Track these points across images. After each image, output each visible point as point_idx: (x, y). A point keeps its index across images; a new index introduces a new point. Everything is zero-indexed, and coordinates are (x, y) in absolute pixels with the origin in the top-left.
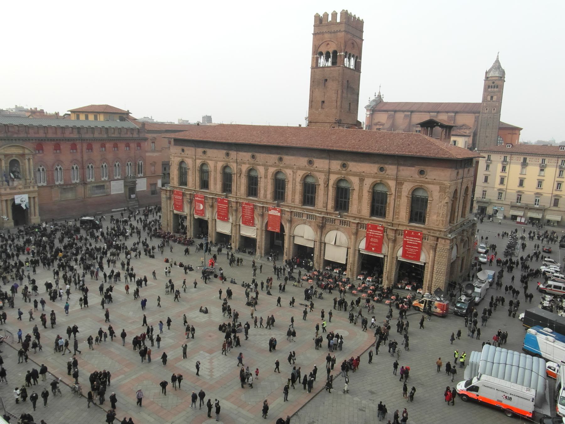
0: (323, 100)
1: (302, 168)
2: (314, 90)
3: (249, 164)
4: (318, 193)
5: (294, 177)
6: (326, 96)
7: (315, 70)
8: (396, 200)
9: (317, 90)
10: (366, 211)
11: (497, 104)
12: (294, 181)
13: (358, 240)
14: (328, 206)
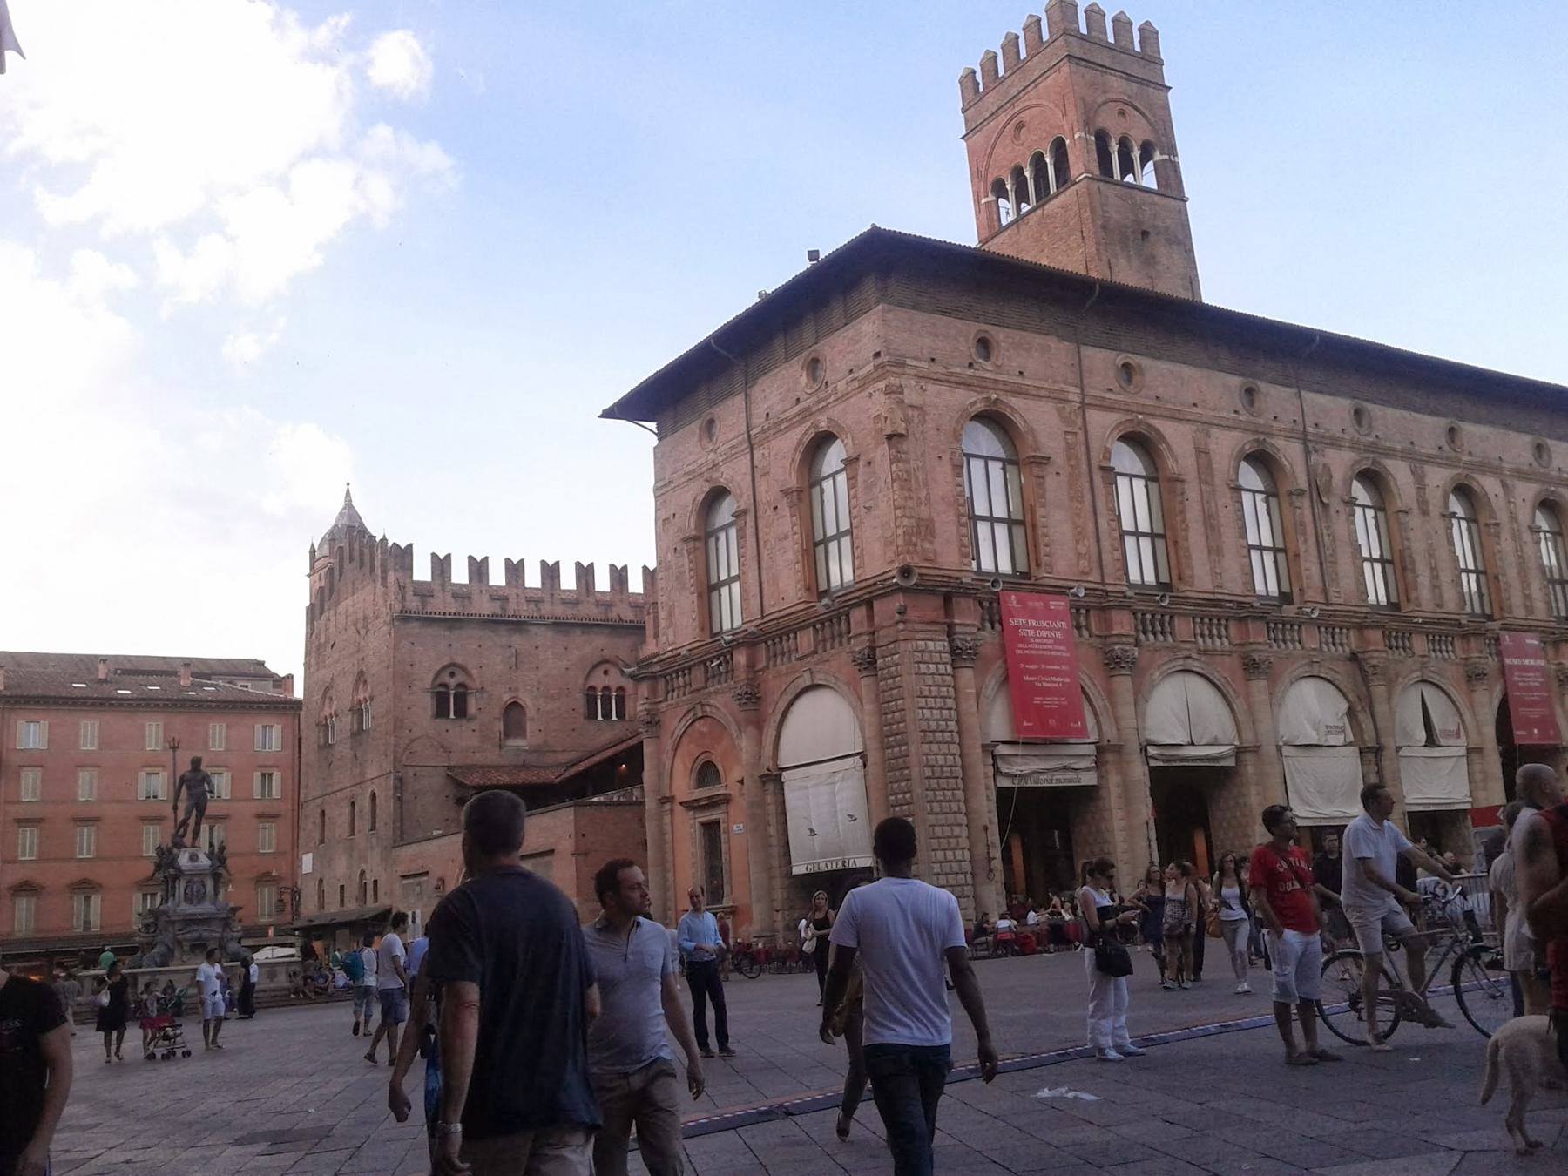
2: (1113, 261)
3: (1354, 446)
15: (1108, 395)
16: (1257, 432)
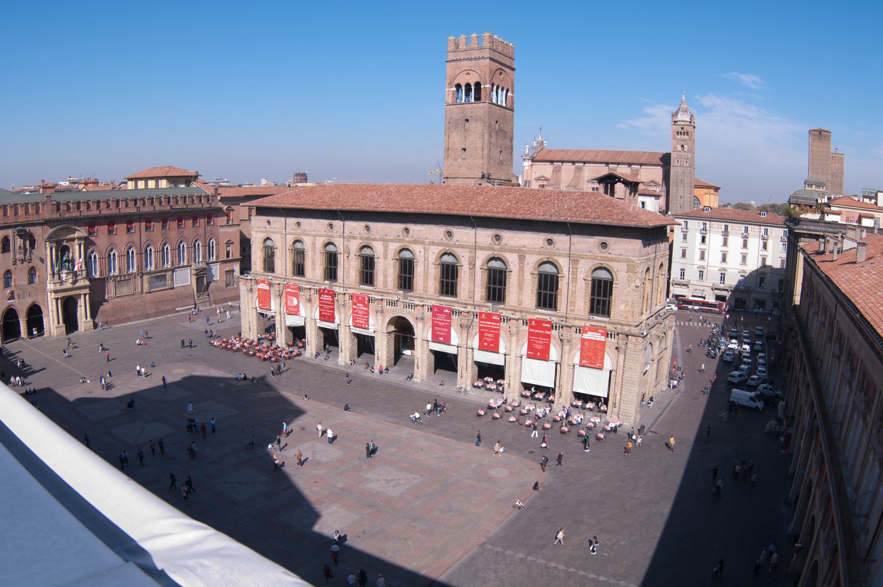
0: (464, 147)
1: (437, 243)
3: (360, 239)
4: (460, 278)
5: (426, 256)
6: (467, 142)
7: (451, 107)
8: (571, 285)
9: (454, 134)
10: (529, 301)
11: (689, 156)
12: (426, 262)
13: (520, 342)
14: (476, 296)
15: (292, 231)
16: (329, 237)
